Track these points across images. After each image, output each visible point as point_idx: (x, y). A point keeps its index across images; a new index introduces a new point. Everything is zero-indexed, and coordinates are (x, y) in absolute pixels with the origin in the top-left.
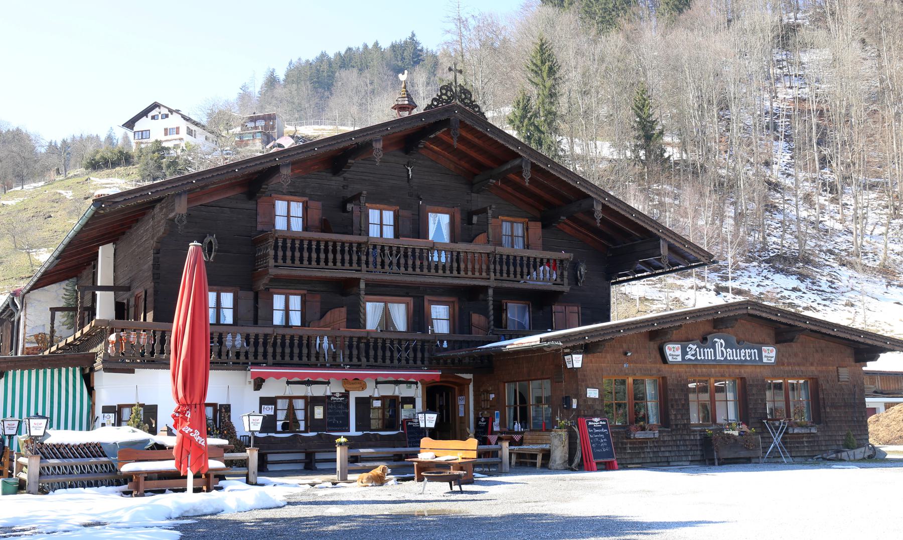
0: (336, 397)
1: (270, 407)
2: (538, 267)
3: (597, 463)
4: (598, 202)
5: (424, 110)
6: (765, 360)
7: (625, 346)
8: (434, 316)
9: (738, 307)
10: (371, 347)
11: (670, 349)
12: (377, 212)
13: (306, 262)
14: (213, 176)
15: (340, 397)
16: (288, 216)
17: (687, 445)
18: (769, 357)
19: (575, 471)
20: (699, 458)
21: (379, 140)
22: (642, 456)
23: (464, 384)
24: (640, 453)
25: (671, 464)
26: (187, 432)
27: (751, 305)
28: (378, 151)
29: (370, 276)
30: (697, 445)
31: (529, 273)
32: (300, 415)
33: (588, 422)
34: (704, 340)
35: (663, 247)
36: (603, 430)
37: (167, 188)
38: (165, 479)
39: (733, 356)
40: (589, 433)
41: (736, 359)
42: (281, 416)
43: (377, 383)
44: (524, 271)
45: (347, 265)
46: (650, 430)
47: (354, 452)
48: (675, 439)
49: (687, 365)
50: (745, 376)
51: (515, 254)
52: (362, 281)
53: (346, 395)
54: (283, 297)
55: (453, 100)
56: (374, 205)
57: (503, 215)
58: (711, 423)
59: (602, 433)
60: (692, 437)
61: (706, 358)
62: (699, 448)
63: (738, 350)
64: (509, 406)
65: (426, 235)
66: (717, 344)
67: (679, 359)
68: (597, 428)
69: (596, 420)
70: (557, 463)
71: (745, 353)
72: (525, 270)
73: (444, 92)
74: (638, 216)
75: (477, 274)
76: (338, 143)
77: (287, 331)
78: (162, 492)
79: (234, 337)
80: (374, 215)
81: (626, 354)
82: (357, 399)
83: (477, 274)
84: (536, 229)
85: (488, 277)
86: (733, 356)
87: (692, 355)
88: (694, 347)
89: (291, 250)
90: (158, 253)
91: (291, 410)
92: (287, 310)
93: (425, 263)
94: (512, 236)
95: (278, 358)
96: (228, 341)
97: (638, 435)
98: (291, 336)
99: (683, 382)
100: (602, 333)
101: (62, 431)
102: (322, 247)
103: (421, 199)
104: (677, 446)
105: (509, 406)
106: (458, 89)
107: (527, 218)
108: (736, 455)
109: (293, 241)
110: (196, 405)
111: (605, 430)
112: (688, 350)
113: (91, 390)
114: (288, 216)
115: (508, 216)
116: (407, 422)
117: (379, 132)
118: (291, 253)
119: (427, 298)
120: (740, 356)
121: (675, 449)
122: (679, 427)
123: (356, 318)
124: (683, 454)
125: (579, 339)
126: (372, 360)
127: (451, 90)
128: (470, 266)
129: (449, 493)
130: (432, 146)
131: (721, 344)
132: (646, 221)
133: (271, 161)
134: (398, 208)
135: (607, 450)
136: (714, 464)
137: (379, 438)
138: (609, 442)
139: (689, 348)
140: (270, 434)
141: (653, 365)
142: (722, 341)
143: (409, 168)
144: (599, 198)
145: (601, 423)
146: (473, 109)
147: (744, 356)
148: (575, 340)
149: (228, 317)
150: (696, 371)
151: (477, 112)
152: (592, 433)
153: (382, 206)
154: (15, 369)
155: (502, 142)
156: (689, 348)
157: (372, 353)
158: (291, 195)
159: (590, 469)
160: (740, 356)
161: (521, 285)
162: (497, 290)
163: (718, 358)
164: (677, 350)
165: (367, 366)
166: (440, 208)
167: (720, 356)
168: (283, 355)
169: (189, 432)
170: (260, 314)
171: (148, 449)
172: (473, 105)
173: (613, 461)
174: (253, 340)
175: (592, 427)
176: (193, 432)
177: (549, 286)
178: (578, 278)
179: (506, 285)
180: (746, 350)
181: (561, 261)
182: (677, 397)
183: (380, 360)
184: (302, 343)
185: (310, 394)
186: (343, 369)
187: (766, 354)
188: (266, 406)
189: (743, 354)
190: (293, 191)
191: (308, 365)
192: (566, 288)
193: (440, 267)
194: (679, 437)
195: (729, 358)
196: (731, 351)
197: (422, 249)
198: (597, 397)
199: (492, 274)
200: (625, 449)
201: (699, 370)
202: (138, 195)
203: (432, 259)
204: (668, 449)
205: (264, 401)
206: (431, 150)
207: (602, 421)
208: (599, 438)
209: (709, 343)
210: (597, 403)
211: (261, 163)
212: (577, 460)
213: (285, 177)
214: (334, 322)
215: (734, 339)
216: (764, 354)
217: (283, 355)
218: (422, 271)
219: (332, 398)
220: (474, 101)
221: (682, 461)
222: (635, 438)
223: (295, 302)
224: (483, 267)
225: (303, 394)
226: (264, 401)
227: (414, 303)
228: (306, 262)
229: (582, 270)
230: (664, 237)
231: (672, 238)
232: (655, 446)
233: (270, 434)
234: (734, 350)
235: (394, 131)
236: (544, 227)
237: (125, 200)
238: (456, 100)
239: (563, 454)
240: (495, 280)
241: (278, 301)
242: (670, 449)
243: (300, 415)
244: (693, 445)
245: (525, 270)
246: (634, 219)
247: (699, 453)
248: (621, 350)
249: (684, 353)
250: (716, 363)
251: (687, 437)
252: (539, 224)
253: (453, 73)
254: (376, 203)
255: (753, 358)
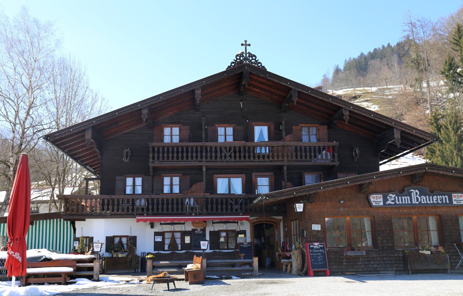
0: (198, 231)
1: (160, 237)
2: (322, 151)
3: (314, 272)
4: (346, 110)
5: (226, 69)
6: (455, 203)
7: (340, 197)
8: (259, 183)
9: (417, 168)
10: (210, 203)
11: (374, 198)
12: (223, 129)
13: (170, 159)
14: (105, 118)
15: (200, 231)
16: (171, 135)
17: (391, 260)
18: (459, 200)
19: (302, 276)
20: (402, 269)
21: (199, 89)
22: (356, 267)
23: (278, 222)
24: (354, 265)
25: (380, 272)
26: (11, 254)
27: (428, 166)
28: (198, 95)
29: (208, 164)
30: (400, 260)
31: (315, 157)
32: (178, 241)
33: (309, 245)
34: (401, 192)
35: (396, 133)
36: (320, 251)
37: (81, 127)
38: (52, 277)
39: (426, 201)
40: (310, 252)
41: (429, 202)
42: (167, 242)
43: (213, 223)
44: (307, 155)
45: (194, 159)
46: (359, 250)
47: (156, 263)
48: (381, 256)
49: (391, 207)
50: (440, 213)
51: (310, 145)
52: (203, 167)
53: (204, 230)
54: (169, 178)
55: (244, 61)
56: (220, 125)
57: (302, 123)
58: (414, 245)
59: (319, 252)
60: (396, 255)
61: (404, 203)
62: (402, 262)
63: (431, 197)
64: (294, 235)
65: (252, 139)
66: (412, 194)
67: (381, 204)
68: (316, 249)
69: (316, 244)
70: (294, 271)
71: (437, 198)
72: (313, 154)
73: (238, 57)
74: (375, 115)
75: (276, 159)
76: (174, 93)
77: (134, 197)
78: (43, 284)
79: (140, 201)
80: (221, 130)
81: (340, 202)
82: (211, 232)
83: (276, 159)
84: (324, 129)
85: (283, 160)
86: (426, 201)
87: (392, 201)
88: (393, 196)
89: (196, 153)
90: (102, 160)
91: (173, 239)
92: (171, 185)
93: (252, 154)
94: (309, 135)
95: (155, 211)
96: (137, 203)
97: (350, 254)
98: (132, 199)
99: (387, 219)
100: (307, 190)
101: (33, 250)
102: (185, 150)
103: (248, 119)
104: (384, 260)
105: (294, 235)
106: (248, 55)
107: (318, 124)
108: (427, 268)
109: (173, 148)
110: (17, 239)
111: (322, 251)
112: (388, 198)
113: (75, 230)
114: (171, 135)
115: (305, 123)
116: (240, 245)
117: (198, 85)
118: (234, 154)
119: (254, 174)
120: (433, 200)
121: (382, 262)
122: (385, 248)
123: (212, 187)
124: (389, 266)
125: (290, 194)
126: (210, 210)
127: (243, 56)
128: (275, 154)
129: (166, 290)
130: (254, 89)
131: (416, 193)
132: (382, 118)
133: (136, 107)
134: (235, 125)
135: (322, 263)
136: (408, 274)
137: (221, 254)
138: (324, 259)
139: (389, 197)
140: (160, 252)
141: (363, 208)
142: (417, 191)
143: (241, 103)
144: (346, 108)
145: (320, 246)
146: (257, 65)
147: (436, 201)
148: (287, 195)
149: (139, 190)
150: (399, 212)
151: (260, 66)
152: (312, 253)
153: (225, 125)
154: (39, 219)
155: (277, 81)
156: (389, 197)
157: (210, 206)
158: (172, 124)
159: (310, 276)
160: (433, 200)
161: (312, 163)
162: (208, 168)
163: (413, 202)
164: (380, 198)
165: (207, 213)
166: (261, 123)
167: (416, 201)
168: (158, 209)
169: (12, 254)
170: (154, 188)
171: (42, 261)
172: (257, 63)
173: (326, 270)
174: (215, 201)
175: (312, 248)
176: (14, 254)
177: (328, 163)
178: (353, 157)
179: (294, 163)
180: (438, 197)
181: (333, 147)
182: (383, 228)
183: (215, 210)
184: (174, 203)
185: (183, 230)
186: (192, 216)
187: (456, 199)
188: (157, 237)
189: (434, 200)
190: (173, 122)
191: (182, 214)
192: (337, 163)
193: (261, 156)
194: (385, 255)
195: (423, 202)
196: (425, 198)
197: (226, 147)
198: (320, 229)
199: (285, 158)
200: (342, 262)
201: (401, 211)
202: (66, 131)
203: (256, 151)
204: (376, 262)
205: (156, 234)
206: (254, 91)
207: (321, 245)
208: (317, 256)
209: (405, 192)
210: (320, 234)
211: (131, 109)
212: (305, 269)
213: (145, 114)
214: (197, 190)
215: (427, 190)
216: (454, 198)
217: (158, 209)
218: (273, 158)
219: (196, 232)
220: (258, 60)
221: (388, 270)
222: (347, 256)
223: (176, 180)
224: (289, 154)
225: (180, 230)
226: (156, 234)
227: (246, 177)
228: (170, 159)
229: (357, 151)
230: (397, 127)
231: (403, 127)
232: (366, 261)
233: (160, 252)
234: (427, 197)
235: (207, 83)
236: (329, 128)
237: (60, 134)
238: (246, 61)
239: (297, 265)
240: (288, 161)
241: (167, 180)
242: (378, 262)
243: (178, 241)
244: (397, 260)
245: (313, 154)
246: (373, 118)
247: (402, 265)
248: (337, 200)
249: (385, 200)
250: (412, 206)
251: (392, 255)
252: (326, 127)
253: (244, 47)
254: (222, 124)
255: (444, 202)
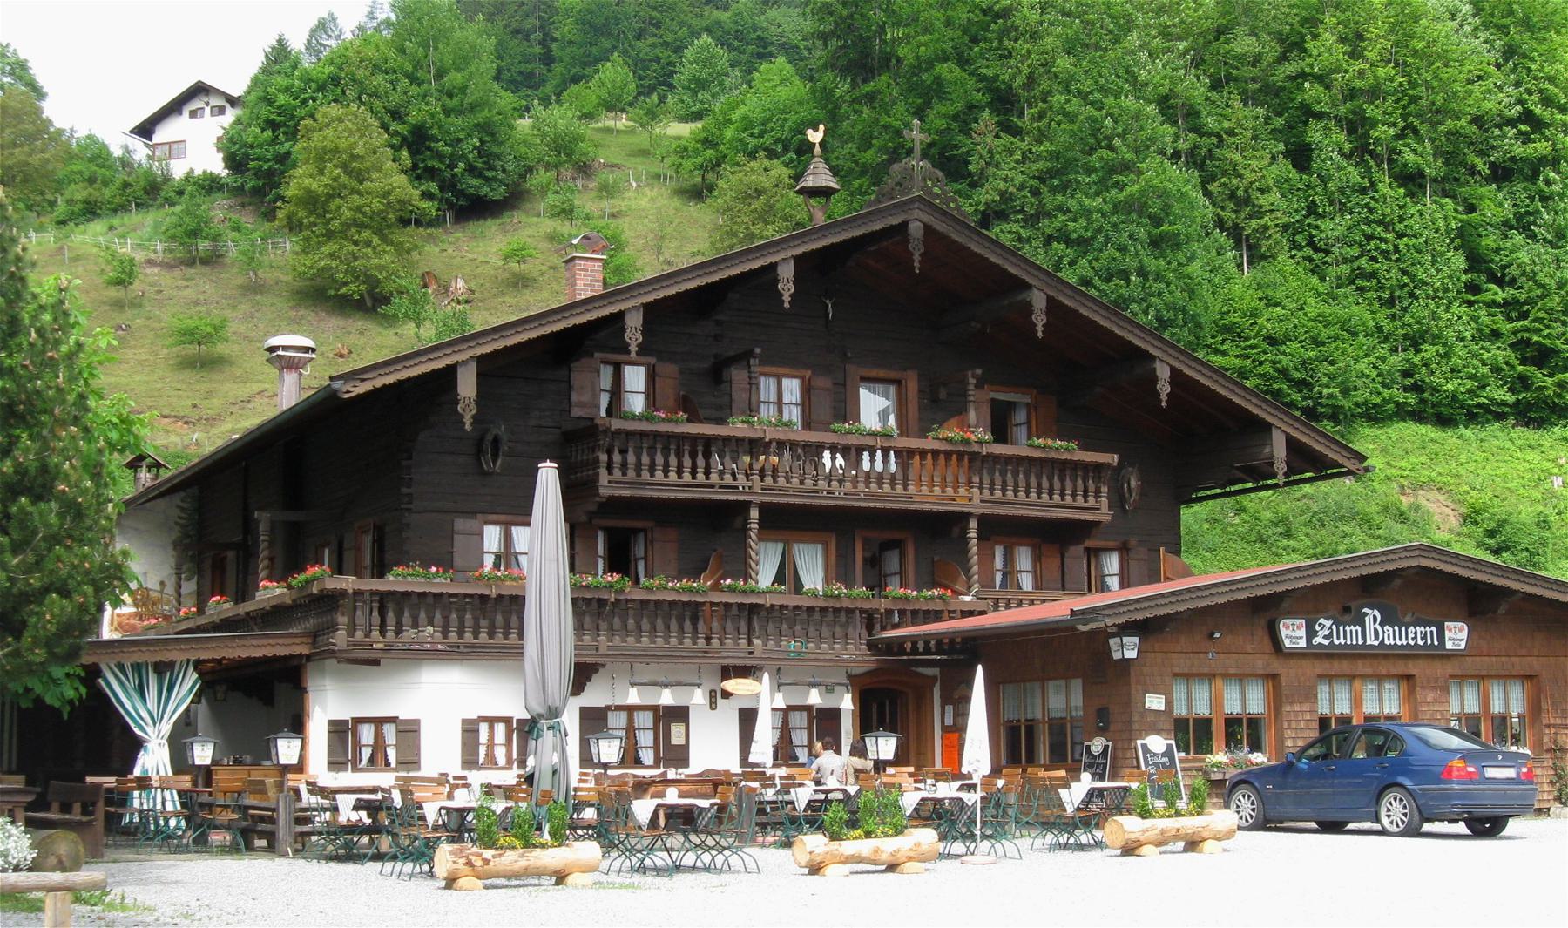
6: (1449, 645)
11: (1287, 627)
12: (772, 382)
41: (1399, 643)
67: (1303, 644)
87: (1325, 637)
88: (1328, 623)
112: (1317, 628)
131: (1375, 617)
142: (1376, 612)
153: (781, 370)
163: (1368, 642)
164: (1299, 628)
189: (1411, 635)
195: (1387, 642)
198: (1163, 708)
216: (1447, 634)
234: (1396, 628)
249: (1311, 633)
